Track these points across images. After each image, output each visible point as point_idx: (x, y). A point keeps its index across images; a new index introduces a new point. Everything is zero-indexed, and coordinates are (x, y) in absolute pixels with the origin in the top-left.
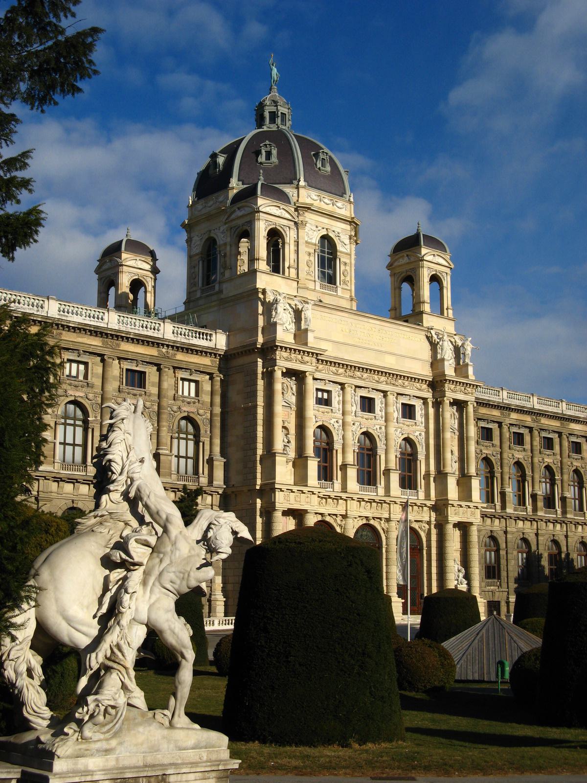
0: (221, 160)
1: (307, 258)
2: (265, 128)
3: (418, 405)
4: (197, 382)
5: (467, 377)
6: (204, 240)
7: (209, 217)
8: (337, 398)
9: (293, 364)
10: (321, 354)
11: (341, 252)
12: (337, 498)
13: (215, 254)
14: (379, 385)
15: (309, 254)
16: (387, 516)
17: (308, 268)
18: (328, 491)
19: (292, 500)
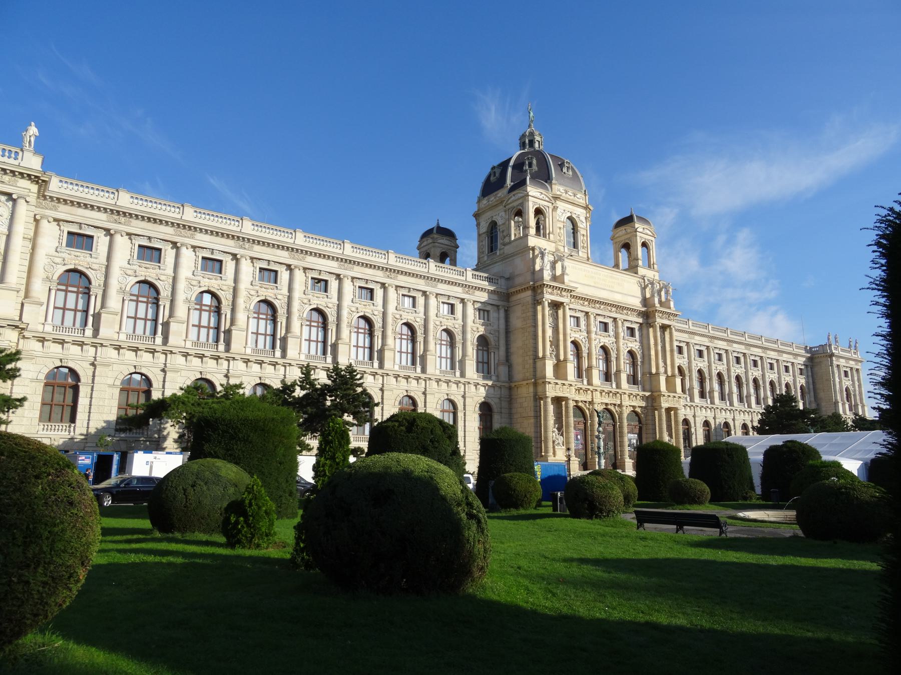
0: (498, 171)
1: (558, 230)
4: (488, 311)
6: (488, 223)
8: (584, 322)
11: (581, 228)
12: (587, 390)
13: (496, 232)
15: (560, 228)
16: (619, 403)
18: (580, 385)
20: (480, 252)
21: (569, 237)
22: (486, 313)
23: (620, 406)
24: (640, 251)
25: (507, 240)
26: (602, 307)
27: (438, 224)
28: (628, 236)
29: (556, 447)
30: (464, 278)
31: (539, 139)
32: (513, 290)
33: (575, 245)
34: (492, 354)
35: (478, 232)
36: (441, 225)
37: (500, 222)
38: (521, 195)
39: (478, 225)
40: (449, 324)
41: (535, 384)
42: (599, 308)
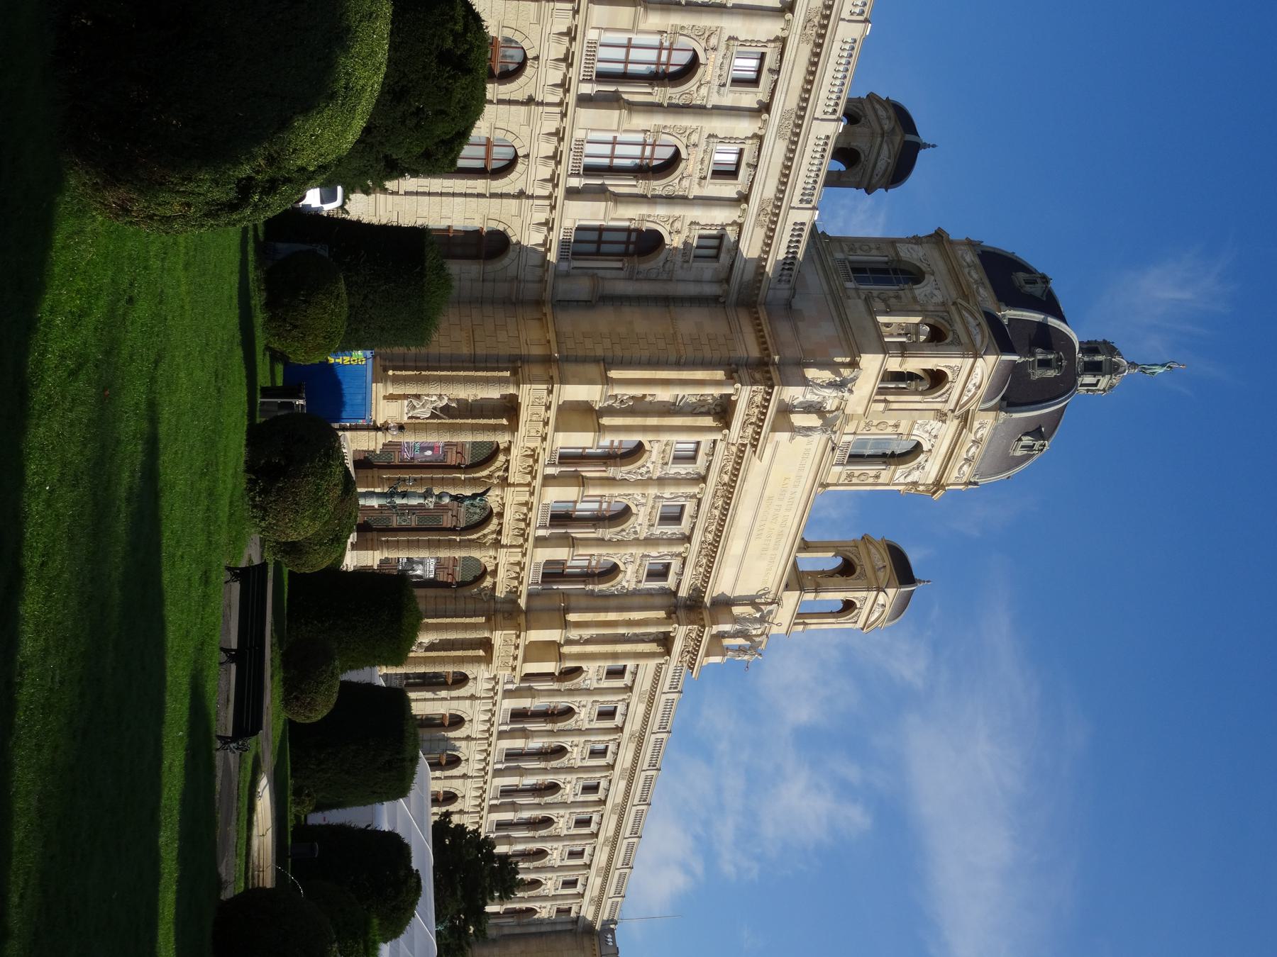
0: (1037, 290)
1: (892, 422)
4: (717, 257)
5: (708, 654)
7: (955, 274)
8: (683, 472)
9: (743, 409)
10: (755, 452)
11: (894, 471)
12: (532, 473)
13: (899, 282)
14: (701, 532)
15: (896, 426)
16: (504, 541)
17: (875, 422)
18: (544, 458)
22: (712, 252)
23: (497, 544)
24: (835, 597)
25: (878, 305)
26: (717, 512)
27: (926, 146)
28: (869, 572)
29: (406, 402)
30: (795, 203)
31: (1102, 385)
32: (763, 315)
33: (856, 458)
34: (619, 265)
37: (921, 291)
38: (978, 339)
39: (917, 240)
40: (692, 165)
41: (547, 360)
42: (713, 506)
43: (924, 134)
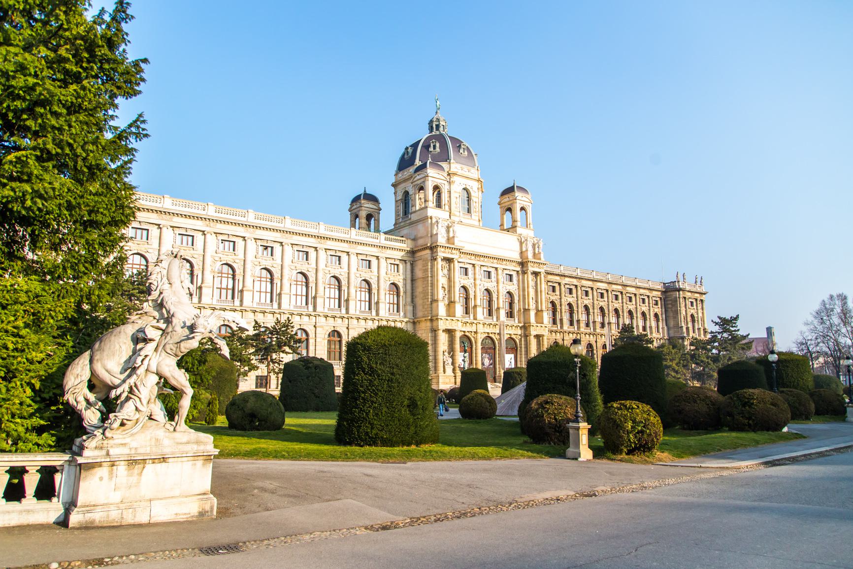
0: (410, 150)
2: (433, 133)
3: (514, 274)
4: (397, 265)
5: (540, 259)
7: (405, 180)
12: (472, 323)
13: (409, 200)
18: (467, 320)
19: (448, 325)
20: (397, 215)
21: (464, 204)
22: (396, 266)
24: (519, 215)
25: (414, 209)
27: (365, 191)
29: (446, 366)
30: (378, 241)
31: (444, 124)
33: (469, 211)
35: (395, 199)
36: (368, 192)
37: (411, 193)
38: (424, 176)
39: (395, 193)
43: (362, 192)
